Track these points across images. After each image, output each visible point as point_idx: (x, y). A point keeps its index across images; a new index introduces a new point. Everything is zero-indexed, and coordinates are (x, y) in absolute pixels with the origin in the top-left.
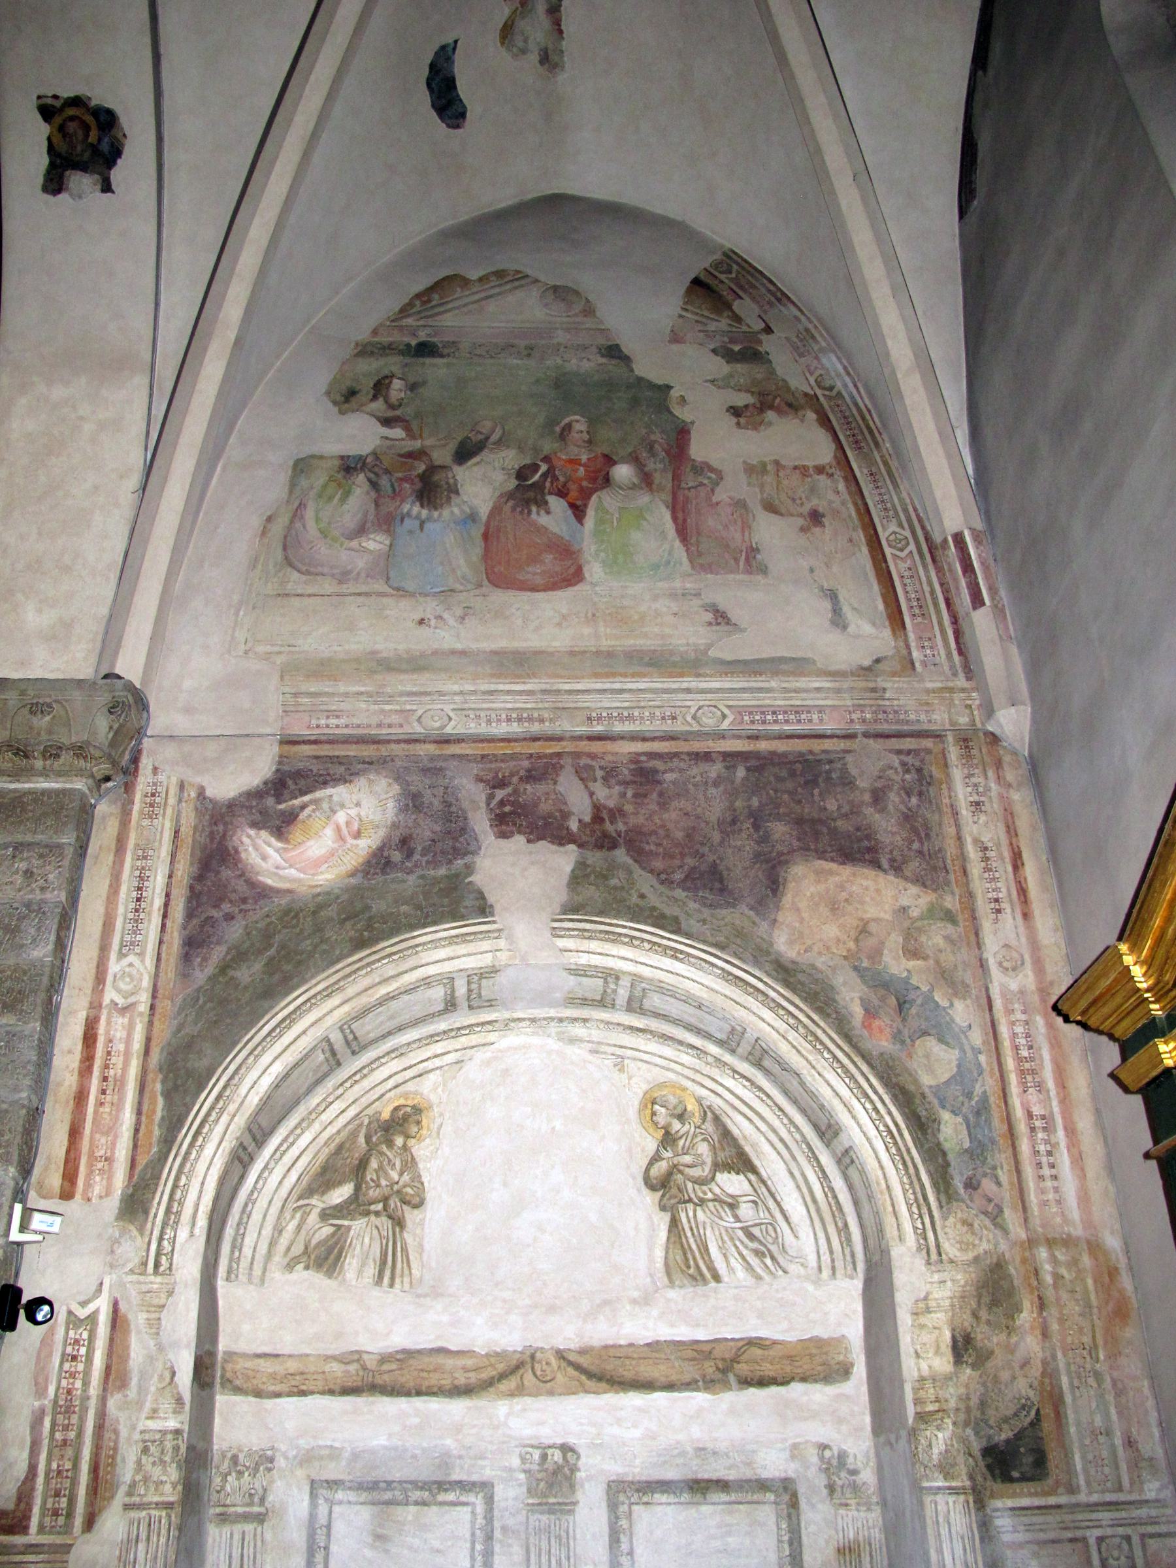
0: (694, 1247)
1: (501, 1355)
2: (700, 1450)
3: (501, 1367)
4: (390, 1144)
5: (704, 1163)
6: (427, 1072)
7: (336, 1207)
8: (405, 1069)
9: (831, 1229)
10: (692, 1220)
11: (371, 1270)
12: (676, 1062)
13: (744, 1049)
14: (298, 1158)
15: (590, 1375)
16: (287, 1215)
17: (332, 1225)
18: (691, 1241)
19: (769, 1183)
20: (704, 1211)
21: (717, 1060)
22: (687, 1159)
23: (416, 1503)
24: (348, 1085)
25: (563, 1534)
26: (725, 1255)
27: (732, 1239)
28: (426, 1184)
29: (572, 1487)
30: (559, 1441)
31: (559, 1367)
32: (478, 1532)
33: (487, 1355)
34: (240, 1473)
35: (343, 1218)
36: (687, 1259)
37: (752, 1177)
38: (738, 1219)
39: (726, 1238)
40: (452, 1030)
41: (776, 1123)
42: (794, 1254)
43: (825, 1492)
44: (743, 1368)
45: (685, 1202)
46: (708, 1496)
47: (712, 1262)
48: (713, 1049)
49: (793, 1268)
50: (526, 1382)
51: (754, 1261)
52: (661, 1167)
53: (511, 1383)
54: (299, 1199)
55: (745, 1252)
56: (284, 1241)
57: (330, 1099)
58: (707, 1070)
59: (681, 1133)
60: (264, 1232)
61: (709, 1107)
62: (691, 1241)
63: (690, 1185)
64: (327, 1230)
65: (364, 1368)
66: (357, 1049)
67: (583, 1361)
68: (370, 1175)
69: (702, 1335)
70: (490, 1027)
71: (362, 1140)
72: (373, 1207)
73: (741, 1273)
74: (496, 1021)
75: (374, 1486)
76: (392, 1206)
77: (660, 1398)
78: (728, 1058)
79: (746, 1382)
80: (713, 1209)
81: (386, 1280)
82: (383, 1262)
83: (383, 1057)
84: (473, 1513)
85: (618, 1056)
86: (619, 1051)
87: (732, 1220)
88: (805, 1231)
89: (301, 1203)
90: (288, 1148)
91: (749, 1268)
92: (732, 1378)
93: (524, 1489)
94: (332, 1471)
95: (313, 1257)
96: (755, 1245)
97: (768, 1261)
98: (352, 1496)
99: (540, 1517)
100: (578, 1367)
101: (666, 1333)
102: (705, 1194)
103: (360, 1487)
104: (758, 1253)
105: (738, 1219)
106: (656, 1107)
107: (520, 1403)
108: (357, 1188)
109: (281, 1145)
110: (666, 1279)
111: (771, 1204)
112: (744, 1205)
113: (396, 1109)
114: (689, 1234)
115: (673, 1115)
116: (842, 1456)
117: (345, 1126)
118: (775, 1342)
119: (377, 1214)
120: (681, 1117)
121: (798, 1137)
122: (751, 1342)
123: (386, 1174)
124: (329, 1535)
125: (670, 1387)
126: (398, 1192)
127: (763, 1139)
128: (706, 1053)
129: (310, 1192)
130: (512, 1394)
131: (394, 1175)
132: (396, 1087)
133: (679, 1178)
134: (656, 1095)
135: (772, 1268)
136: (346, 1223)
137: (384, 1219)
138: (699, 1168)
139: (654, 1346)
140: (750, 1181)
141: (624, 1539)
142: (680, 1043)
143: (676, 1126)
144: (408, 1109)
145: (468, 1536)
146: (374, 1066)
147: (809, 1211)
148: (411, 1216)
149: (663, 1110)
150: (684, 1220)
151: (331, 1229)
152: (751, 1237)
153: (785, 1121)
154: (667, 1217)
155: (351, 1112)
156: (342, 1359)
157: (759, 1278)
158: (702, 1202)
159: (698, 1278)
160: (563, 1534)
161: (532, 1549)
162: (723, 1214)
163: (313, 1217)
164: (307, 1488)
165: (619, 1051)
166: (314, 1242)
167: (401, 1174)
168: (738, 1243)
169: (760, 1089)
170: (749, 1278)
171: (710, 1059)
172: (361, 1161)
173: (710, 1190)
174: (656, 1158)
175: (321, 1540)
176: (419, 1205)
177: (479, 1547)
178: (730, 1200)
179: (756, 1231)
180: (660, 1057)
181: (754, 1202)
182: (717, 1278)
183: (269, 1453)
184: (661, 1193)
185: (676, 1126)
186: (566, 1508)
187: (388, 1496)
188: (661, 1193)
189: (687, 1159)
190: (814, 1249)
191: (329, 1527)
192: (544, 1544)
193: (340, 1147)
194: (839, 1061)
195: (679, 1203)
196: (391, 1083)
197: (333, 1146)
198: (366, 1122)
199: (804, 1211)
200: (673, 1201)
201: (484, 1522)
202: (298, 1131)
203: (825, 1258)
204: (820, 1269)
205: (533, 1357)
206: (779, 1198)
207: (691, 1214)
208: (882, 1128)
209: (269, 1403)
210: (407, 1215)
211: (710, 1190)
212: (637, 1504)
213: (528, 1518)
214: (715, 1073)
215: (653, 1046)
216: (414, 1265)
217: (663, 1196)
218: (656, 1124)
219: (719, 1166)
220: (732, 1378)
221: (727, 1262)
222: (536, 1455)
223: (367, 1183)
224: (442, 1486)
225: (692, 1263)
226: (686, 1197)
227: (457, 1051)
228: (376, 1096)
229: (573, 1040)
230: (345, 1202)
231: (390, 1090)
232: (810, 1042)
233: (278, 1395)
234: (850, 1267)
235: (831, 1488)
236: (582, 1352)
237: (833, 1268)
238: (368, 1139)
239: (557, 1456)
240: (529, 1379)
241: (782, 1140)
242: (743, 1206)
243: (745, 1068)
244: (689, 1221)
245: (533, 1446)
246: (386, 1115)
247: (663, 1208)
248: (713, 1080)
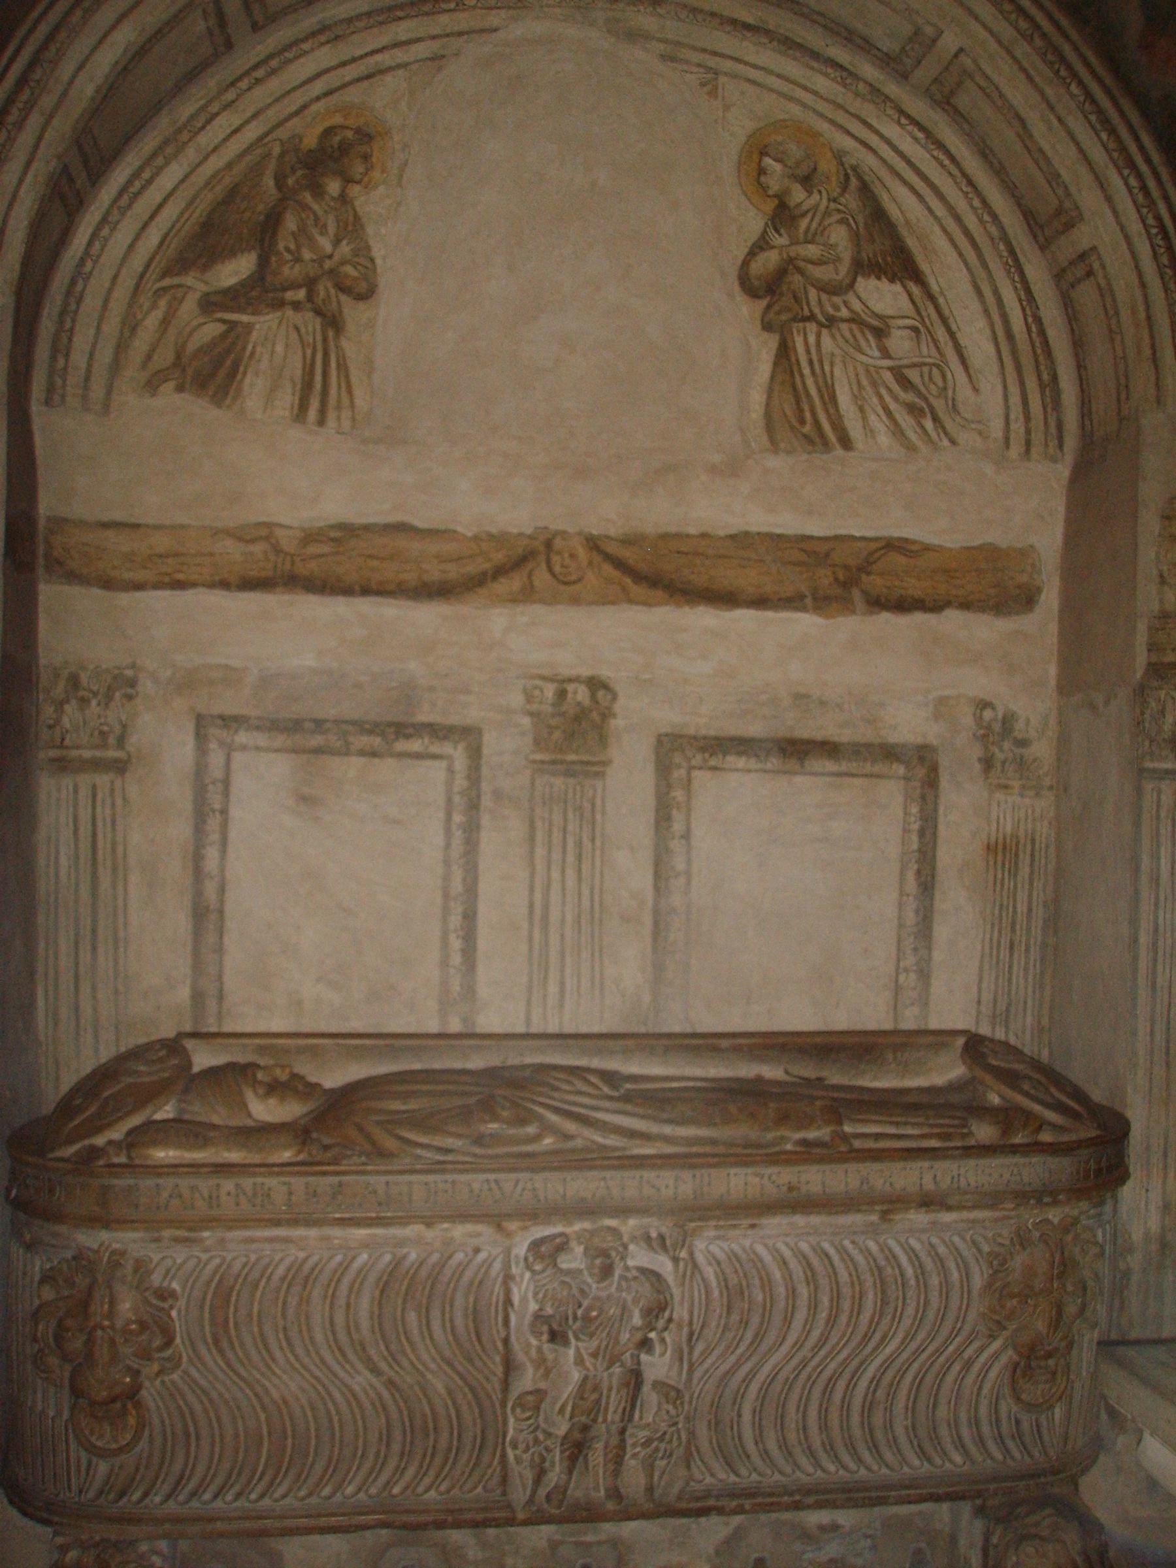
0: (813, 391)
1: (500, 539)
2: (801, 698)
3: (499, 557)
4: (318, 191)
5: (838, 259)
6: (382, 72)
7: (226, 292)
8: (343, 64)
9: (1032, 384)
10: (813, 350)
11: (287, 399)
12: (806, 88)
14: (161, 206)
15: (638, 577)
16: (145, 300)
17: (224, 321)
18: (810, 382)
19: (941, 300)
20: (833, 337)
21: (875, 90)
22: (812, 251)
23: (362, 753)
24: (244, 84)
25: (587, 806)
26: (861, 409)
27: (874, 384)
28: (379, 262)
29: (603, 741)
30: (586, 672)
31: (590, 563)
32: (457, 799)
33: (476, 538)
34: (84, 702)
36: (801, 411)
37: (915, 290)
38: (886, 353)
39: (865, 382)
41: (961, 205)
42: (968, 416)
43: (978, 767)
44: (875, 583)
46: (807, 763)
47: (840, 417)
48: (869, 70)
49: (963, 437)
50: (536, 583)
51: (905, 420)
52: (769, 260)
53: (514, 583)
54: (163, 276)
55: (893, 406)
56: (140, 344)
57: (215, 108)
58: (856, 105)
59: (804, 207)
60: (106, 328)
62: (810, 382)
63: (813, 293)
64: (212, 330)
65: (277, 550)
67: (628, 555)
69: (815, 528)
71: (269, 182)
72: (289, 295)
73: (884, 439)
75: (295, 726)
76: (322, 294)
77: (745, 617)
78: (892, 89)
79: (877, 603)
80: (848, 335)
81: (312, 414)
82: (308, 386)
83: (305, 39)
84: (450, 771)
85: (709, 69)
86: (712, 62)
87: (877, 354)
88: (990, 384)
89: (167, 282)
90: (144, 188)
91: (897, 431)
92: (856, 594)
93: (529, 739)
94: (228, 704)
95: (190, 371)
96: (910, 397)
97: (929, 424)
98: (261, 739)
99: (552, 780)
100: (619, 564)
101: (758, 520)
102: (837, 309)
103: (274, 726)
104: (911, 409)
105: (886, 353)
106: (768, 161)
107: (526, 614)
108: (263, 262)
109: (129, 182)
110: (765, 438)
111: (941, 334)
112: (899, 333)
113: (328, 132)
114: (807, 371)
115: (794, 177)
116: (1008, 720)
118: (927, 548)
119: (296, 306)
120: (807, 181)
121: (993, 230)
122: (892, 545)
123: (311, 239)
124: (226, 793)
125: (761, 602)
126: (331, 272)
127: (937, 230)
129: (182, 263)
130: (514, 600)
131: (325, 244)
132: (328, 93)
135: (933, 434)
136: (245, 318)
137: (310, 315)
138: (831, 267)
139: (742, 539)
140: (910, 295)
141: (678, 817)
142: (815, 55)
143: (798, 195)
144: (349, 134)
145: (441, 801)
147: (999, 352)
148: (353, 313)
149: (778, 167)
151: (221, 328)
152: (905, 383)
153: (976, 203)
154: (773, 341)
155: (251, 133)
156: (240, 535)
157: (911, 448)
158: (831, 322)
159: (816, 441)
160: (587, 806)
161: (539, 824)
162: (863, 343)
163: (189, 306)
164: (191, 726)
165: (712, 62)
166: (191, 347)
167: (337, 242)
168: (883, 392)
169: (940, 145)
171: (861, 86)
172: (268, 216)
173: (846, 303)
174: (761, 245)
175: (215, 799)
176: (366, 294)
177: (457, 818)
178: (875, 323)
179: (913, 375)
180: (779, 76)
181: (915, 330)
182: (846, 442)
183: (129, 673)
184: (764, 302)
185: (798, 195)
186: (595, 769)
187: (317, 740)
188: (764, 302)
189: (812, 251)
190: (1000, 411)
191: (226, 782)
192: (557, 818)
194: (1094, 101)
195: (795, 319)
196: (318, 87)
197: (219, 190)
198: (277, 150)
199: (992, 350)
200: (784, 317)
201: (465, 783)
203: (1018, 427)
204: (1007, 440)
205: (549, 544)
206: (954, 327)
207: (812, 339)
208: (1151, 221)
209: (124, 599)
210: (346, 311)
211: (846, 303)
212: (700, 768)
213: (533, 784)
214: (869, 111)
215: (768, 57)
216: (358, 392)
217: (769, 307)
218: (763, 188)
219: (861, 267)
220: (856, 594)
221: (864, 419)
222: (550, 691)
223: (278, 253)
224: (403, 730)
225: (808, 415)
226: (806, 312)
227: (434, 38)
228: (294, 108)
229: (634, 36)
230: (242, 284)
231: (318, 99)
232: (1051, 64)
233: (139, 587)
234: (1053, 443)
235: (988, 763)
236: (628, 541)
237: (1028, 444)
239: (581, 694)
240: (542, 577)
241: (967, 233)
242: (897, 333)
243: (918, 107)
244: (808, 352)
245: (543, 678)
246: (311, 141)
247: (767, 327)
248: (865, 123)
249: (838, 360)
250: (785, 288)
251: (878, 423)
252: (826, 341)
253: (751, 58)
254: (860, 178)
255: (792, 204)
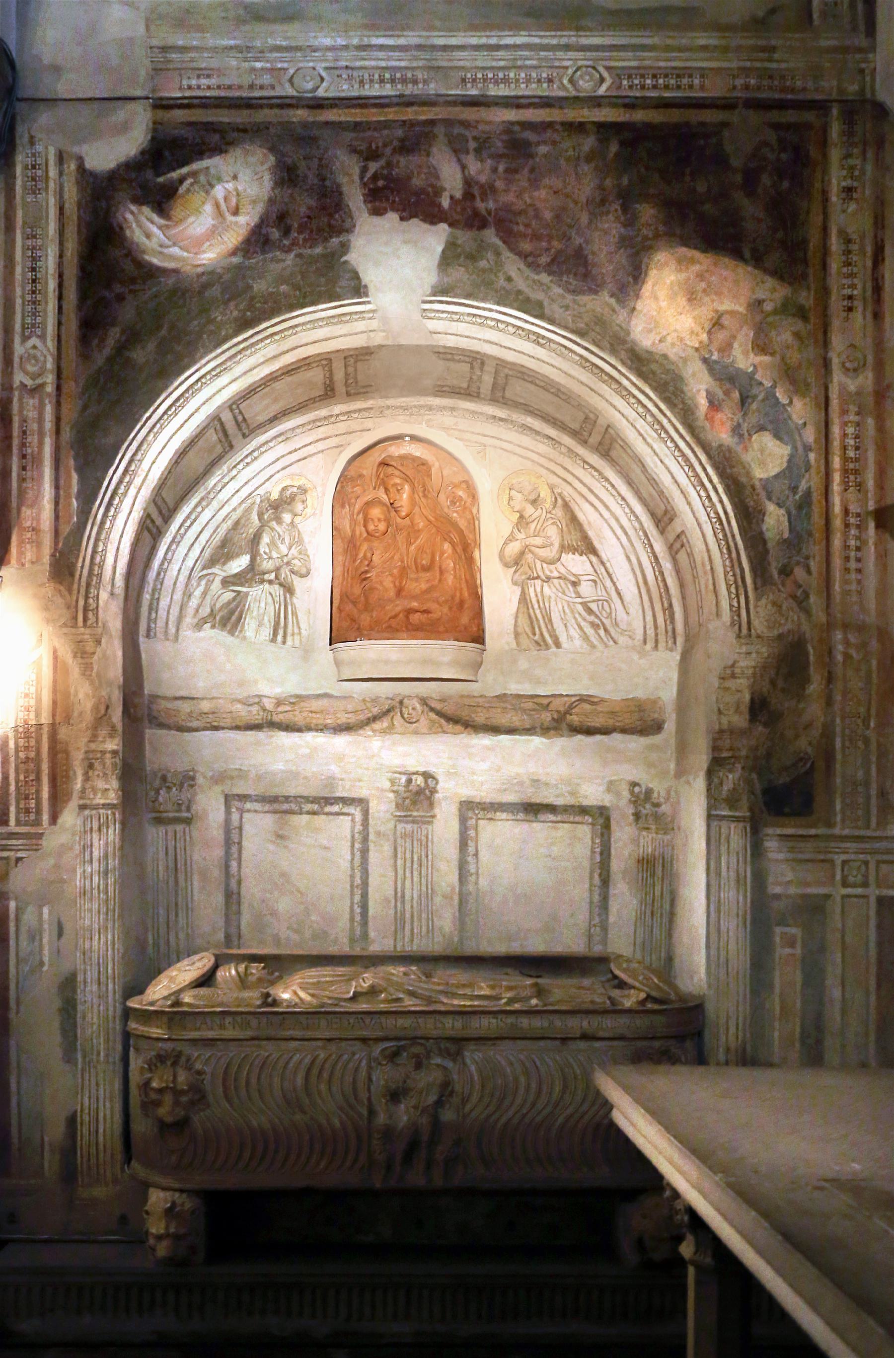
4: (279, 520)
13: (594, 439)
16: (194, 582)
18: (538, 612)
19: (608, 565)
22: (538, 541)
24: (240, 467)
26: (565, 625)
27: (572, 612)
35: (242, 585)
36: (533, 628)
37: (594, 559)
39: (567, 611)
40: (332, 416)
45: (534, 578)
47: (554, 631)
48: (567, 440)
52: (514, 548)
54: (204, 568)
55: (583, 624)
58: (561, 459)
59: (534, 517)
61: (560, 494)
62: (538, 612)
64: (229, 596)
66: (246, 431)
68: (263, 548)
70: (366, 414)
71: (255, 517)
72: (266, 577)
73: (578, 642)
74: (371, 408)
78: (581, 450)
83: (270, 441)
89: (205, 572)
90: (192, 524)
91: (586, 638)
95: (218, 618)
96: (592, 618)
104: (594, 625)
109: (185, 521)
113: (284, 489)
114: (536, 606)
117: (240, 504)
119: (270, 582)
120: (534, 502)
126: (288, 563)
128: (560, 443)
133: (529, 557)
134: (514, 481)
135: (605, 639)
137: (277, 587)
142: (537, 433)
144: (295, 490)
146: (263, 449)
149: (519, 495)
150: (532, 594)
151: (234, 594)
152: (590, 611)
153: (627, 510)
154: (518, 591)
163: (217, 584)
166: (218, 606)
167: (290, 548)
170: (585, 646)
171: (563, 449)
174: (511, 539)
178: (573, 579)
179: (593, 606)
181: (594, 581)
182: (558, 645)
185: (530, 510)
189: (538, 541)
193: (237, 523)
198: (258, 500)
202: (199, 509)
217: (515, 572)
221: (567, 631)
223: (260, 555)
225: (537, 630)
230: (242, 572)
238: (260, 515)
241: (622, 527)
246: (275, 496)
248: (565, 469)
249: (552, 600)
250: (523, 562)
251: (574, 633)
252: (546, 589)
253: (503, 437)
254: (563, 499)
255: (527, 516)
